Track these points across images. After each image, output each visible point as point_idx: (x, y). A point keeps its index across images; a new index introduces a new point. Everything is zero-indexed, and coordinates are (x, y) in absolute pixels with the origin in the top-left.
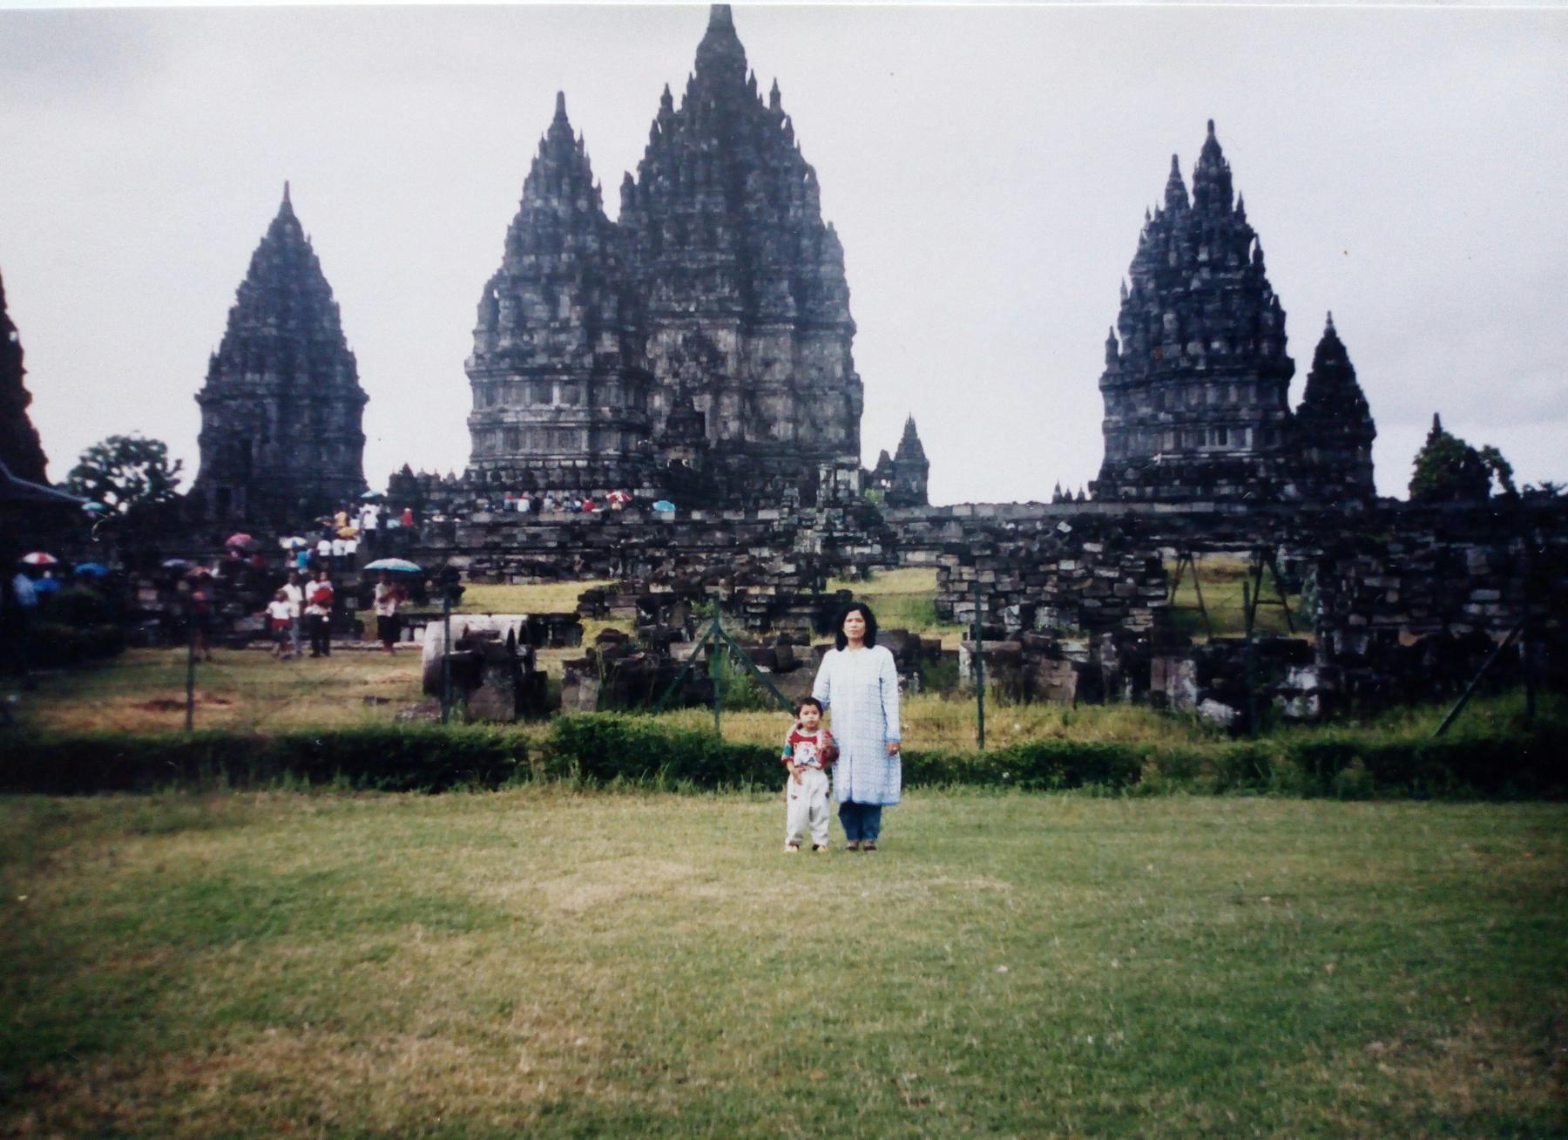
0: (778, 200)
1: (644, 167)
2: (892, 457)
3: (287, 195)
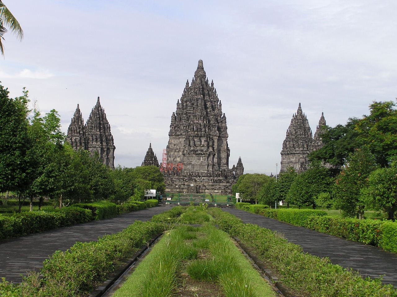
0: (213, 108)
1: (182, 99)
2: (236, 167)
3: (98, 100)
